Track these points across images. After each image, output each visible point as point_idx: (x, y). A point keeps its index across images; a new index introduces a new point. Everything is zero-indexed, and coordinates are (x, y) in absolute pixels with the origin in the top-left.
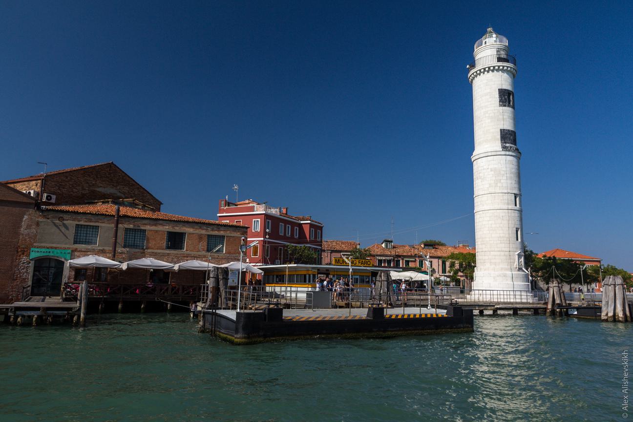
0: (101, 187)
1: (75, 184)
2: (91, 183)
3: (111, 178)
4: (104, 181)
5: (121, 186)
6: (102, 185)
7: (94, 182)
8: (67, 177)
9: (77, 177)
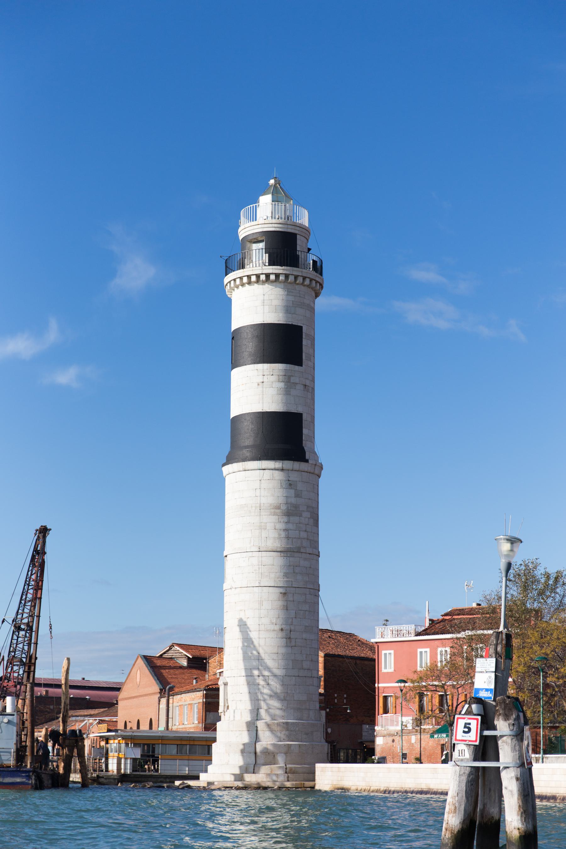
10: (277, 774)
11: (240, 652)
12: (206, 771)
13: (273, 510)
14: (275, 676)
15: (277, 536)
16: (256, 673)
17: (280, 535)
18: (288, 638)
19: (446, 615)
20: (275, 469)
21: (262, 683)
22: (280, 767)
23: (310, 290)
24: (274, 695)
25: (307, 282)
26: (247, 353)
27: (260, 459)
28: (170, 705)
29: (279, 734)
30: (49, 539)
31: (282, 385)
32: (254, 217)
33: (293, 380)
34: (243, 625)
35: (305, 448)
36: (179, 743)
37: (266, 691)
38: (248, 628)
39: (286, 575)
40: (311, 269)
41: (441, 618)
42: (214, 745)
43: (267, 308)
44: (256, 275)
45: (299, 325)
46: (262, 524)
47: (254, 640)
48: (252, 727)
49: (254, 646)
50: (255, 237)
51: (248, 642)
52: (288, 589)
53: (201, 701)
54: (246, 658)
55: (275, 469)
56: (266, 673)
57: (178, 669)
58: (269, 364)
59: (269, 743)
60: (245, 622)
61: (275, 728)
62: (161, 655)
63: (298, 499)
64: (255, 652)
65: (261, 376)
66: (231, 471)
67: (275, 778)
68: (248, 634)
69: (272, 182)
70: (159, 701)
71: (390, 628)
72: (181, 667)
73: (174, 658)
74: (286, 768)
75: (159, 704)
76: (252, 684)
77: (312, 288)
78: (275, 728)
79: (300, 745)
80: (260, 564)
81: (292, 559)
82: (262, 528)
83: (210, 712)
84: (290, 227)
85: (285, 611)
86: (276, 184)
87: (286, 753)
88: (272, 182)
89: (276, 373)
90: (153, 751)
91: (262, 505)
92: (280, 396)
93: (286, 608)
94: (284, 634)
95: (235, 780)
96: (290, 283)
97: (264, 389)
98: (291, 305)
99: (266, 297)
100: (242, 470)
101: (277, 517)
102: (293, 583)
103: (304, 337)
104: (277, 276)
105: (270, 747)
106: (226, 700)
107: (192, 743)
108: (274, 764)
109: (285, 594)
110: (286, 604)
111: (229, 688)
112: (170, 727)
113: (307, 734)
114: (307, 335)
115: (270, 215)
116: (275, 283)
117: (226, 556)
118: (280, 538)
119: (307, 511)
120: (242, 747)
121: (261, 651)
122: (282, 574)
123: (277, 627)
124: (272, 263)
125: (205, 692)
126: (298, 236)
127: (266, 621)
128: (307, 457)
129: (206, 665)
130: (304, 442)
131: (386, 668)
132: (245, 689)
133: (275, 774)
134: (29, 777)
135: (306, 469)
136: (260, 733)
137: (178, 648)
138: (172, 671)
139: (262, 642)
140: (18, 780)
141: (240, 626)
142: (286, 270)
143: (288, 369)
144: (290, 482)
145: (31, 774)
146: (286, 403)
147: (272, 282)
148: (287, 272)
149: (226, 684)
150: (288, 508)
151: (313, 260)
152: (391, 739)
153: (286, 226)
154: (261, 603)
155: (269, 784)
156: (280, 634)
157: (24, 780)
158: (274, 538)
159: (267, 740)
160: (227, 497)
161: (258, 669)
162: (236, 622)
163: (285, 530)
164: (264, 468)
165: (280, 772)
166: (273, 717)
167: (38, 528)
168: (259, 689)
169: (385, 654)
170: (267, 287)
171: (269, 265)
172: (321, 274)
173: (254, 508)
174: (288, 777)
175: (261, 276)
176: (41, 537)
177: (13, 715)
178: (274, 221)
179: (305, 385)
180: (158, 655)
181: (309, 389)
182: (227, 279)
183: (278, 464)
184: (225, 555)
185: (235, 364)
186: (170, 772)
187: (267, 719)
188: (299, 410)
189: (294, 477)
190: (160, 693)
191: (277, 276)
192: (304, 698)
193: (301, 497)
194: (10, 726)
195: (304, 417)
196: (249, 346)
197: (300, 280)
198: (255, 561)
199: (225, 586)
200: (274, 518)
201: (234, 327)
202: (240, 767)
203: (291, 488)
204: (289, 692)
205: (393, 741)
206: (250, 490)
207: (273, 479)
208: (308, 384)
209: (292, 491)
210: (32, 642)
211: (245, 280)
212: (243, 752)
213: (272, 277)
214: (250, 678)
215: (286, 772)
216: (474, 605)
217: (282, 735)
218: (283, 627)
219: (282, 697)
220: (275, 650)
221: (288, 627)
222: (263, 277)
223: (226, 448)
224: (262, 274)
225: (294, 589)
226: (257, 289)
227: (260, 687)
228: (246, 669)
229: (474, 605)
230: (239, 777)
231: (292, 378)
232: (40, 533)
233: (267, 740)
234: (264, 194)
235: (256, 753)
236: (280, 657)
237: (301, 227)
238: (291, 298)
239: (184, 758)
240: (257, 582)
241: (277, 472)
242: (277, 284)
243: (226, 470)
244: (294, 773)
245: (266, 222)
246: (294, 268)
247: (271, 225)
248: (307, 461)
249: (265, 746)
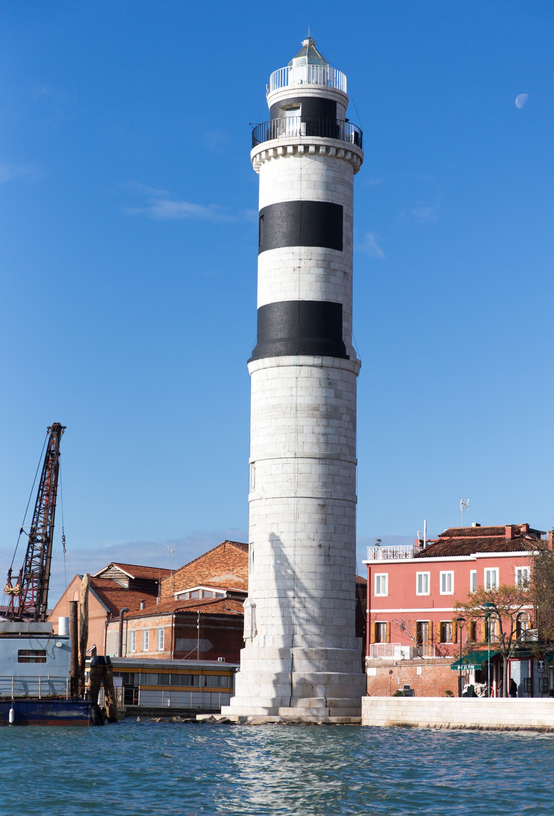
0: (215, 576)
1: (188, 581)
2: (204, 574)
3: (226, 561)
4: (218, 568)
5: (239, 568)
6: (216, 573)
7: (207, 573)
8: (180, 575)
9: (190, 572)
10: (318, 708)
11: (272, 570)
12: (228, 704)
13: (311, 412)
14: (312, 598)
15: (315, 441)
16: (291, 594)
17: (318, 439)
18: (327, 556)
19: (444, 535)
20: (314, 366)
21: (297, 605)
22: (320, 700)
23: (350, 165)
24: (311, 620)
25: (349, 156)
26: (280, 234)
27: (297, 354)
28: (124, 631)
29: (317, 663)
30: (64, 438)
31: (321, 271)
32: (283, 82)
33: (333, 266)
34: (275, 541)
35: (345, 343)
36: (160, 672)
37: (302, 614)
38: (282, 544)
39: (325, 485)
40: (353, 142)
41: (439, 538)
42: (237, 675)
43: (304, 184)
44: (293, 145)
45: (340, 204)
46: (299, 427)
47: (288, 557)
48: (285, 654)
49: (289, 564)
50: (289, 103)
51: (281, 560)
52: (327, 500)
53: (170, 625)
54: (279, 577)
55: (314, 366)
56: (302, 595)
57: (119, 591)
58: (307, 247)
59: (306, 673)
60: (278, 537)
61: (313, 656)
62: (98, 576)
64: (289, 571)
65: (298, 261)
66: (261, 367)
67: (315, 712)
68: (281, 551)
69: (306, 42)
70: (107, 626)
71: (383, 548)
72: (123, 589)
73: (113, 579)
74: (326, 702)
75: (106, 629)
76: (285, 606)
77: (352, 164)
78: (313, 656)
79: (340, 676)
80: (296, 472)
82: (298, 431)
83: (180, 638)
84: (330, 93)
85: (324, 525)
86: (310, 45)
87: (325, 685)
88: (306, 42)
89: (315, 257)
90: (133, 681)
91: (298, 406)
92: (319, 284)
93: (325, 522)
95: (269, 714)
96: (330, 156)
97: (301, 275)
99: (304, 171)
100: (275, 365)
101: (315, 419)
102: (333, 494)
103: (344, 217)
104: (317, 147)
105: (308, 678)
106: (253, 624)
107: (174, 672)
108: (313, 696)
109: (323, 506)
110: (324, 518)
111: (257, 610)
112: (123, 655)
113: (346, 663)
114: (347, 216)
115: (305, 79)
116: (313, 156)
117: (253, 463)
118: (318, 443)
119: (347, 414)
120: (274, 677)
121: (297, 570)
122: (321, 484)
123: (315, 543)
124: (309, 133)
125: (174, 616)
126: (338, 105)
127: (302, 536)
128: (347, 354)
129: (158, 588)
130: (343, 336)
131: (378, 592)
132: (277, 612)
133: (315, 708)
134: (87, 711)
135: (347, 367)
136: (296, 662)
137: (118, 568)
138: (114, 593)
139: (298, 560)
140: (75, 714)
141: (271, 541)
142: (328, 141)
143: (328, 253)
144: (330, 381)
145: (90, 707)
146: (326, 292)
147: (312, 154)
148: (329, 144)
149: (253, 606)
150: (327, 409)
151: (355, 132)
152: (388, 670)
153: (326, 92)
154: (297, 516)
155: (312, 719)
156: (318, 551)
157: (82, 714)
158: (312, 443)
159: (303, 669)
160: (254, 397)
161: (294, 590)
162: (267, 537)
163: (325, 434)
164: (301, 363)
165: (320, 705)
166: (310, 644)
167: (51, 426)
168: (294, 613)
169: (378, 578)
170: (305, 160)
171: (306, 135)
172: (361, 148)
173: (289, 409)
174: (329, 712)
175: (299, 147)
176: (55, 436)
177: (68, 638)
178: (312, 86)
179: (345, 273)
180: (94, 576)
181: (347, 276)
182: (255, 151)
183: (317, 360)
184: (251, 460)
185: (263, 246)
186: (154, 704)
187: (304, 646)
188: (338, 299)
189: (335, 375)
190: (108, 617)
191: (317, 147)
194: (64, 651)
195: (344, 308)
196: (281, 226)
197: (342, 153)
198: (290, 468)
199: (251, 497)
200: (312, 421)
201: (261, 206)
202: (273, 700)
203: (331, 388)
204: (328, 616)
205: (391, 672)
206: (281, 391)
207: (311, 376)
208: (347, 271)
209: (332, 391)
210: (46, 555)
211: (280, 151)
212: (275, 683)
213: (312, 149)
214: (283, 600)
215: (326, 706)
216: (473, 525)
217: (320, 664)
218: (322, 542)
219: (320, 622)
220: (313, 569)
221: (327, 544)
222: (301, 149)
223: (253, 342)
224: (300, 145)
225: (333, 501)
226: (293, 162)
227: (295, 610)
228: (279, 590)
229: (473, 525)
230: (273, 711)
231: (332, 264)
232: (53, 431)
233: (303, 669)
234: (297, 55)
235: (292, 684)
236: (318, 576)
237: (341, 94)
238: (331, 174)
239: (166, 688)
240: (293, 492)
241: (315, 369)
242: (316, 156)
243: (252, 366)
244: (334, 706)
245: (300, 86)
246: (336, 140)
247: (308, 91)
248: (347, 358)
249: (302, 676)
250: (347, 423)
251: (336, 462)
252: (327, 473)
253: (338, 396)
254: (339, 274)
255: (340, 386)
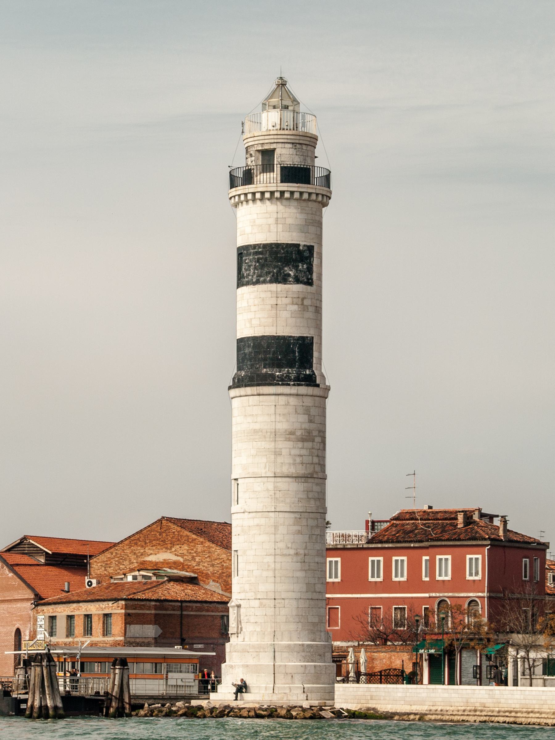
13: (288, 436)
25: (320, 198)
43: (280, 226)
63: (311, 424)
74: (304, 688)
79: (315, 666)
81: (306, 484)
82: (277, 453)
91: (277, 431)
94: (299, 558)
97: (278, 312)
98: (304, 223)
100: (255, 393)
106: (239, 622)
111: (242, 610)
154: (276, 527)
158: (290, 464)
173: (269, 434)
175: (276, 194)
184: (233, 477)
189: (308, 401)
192: (316, 620)
193: (314, 422)
197: (314, 197)
198: (271, 486)
204: (304, 614)
211: (258, 196)
226: (269, 207)
238: (303, 216)
240: (273, 507)
250: (318, 444)
251: (310, 480)
252: (302, 490)
253: (310, 421)
254: (311, 309)
255: (313, 411)
